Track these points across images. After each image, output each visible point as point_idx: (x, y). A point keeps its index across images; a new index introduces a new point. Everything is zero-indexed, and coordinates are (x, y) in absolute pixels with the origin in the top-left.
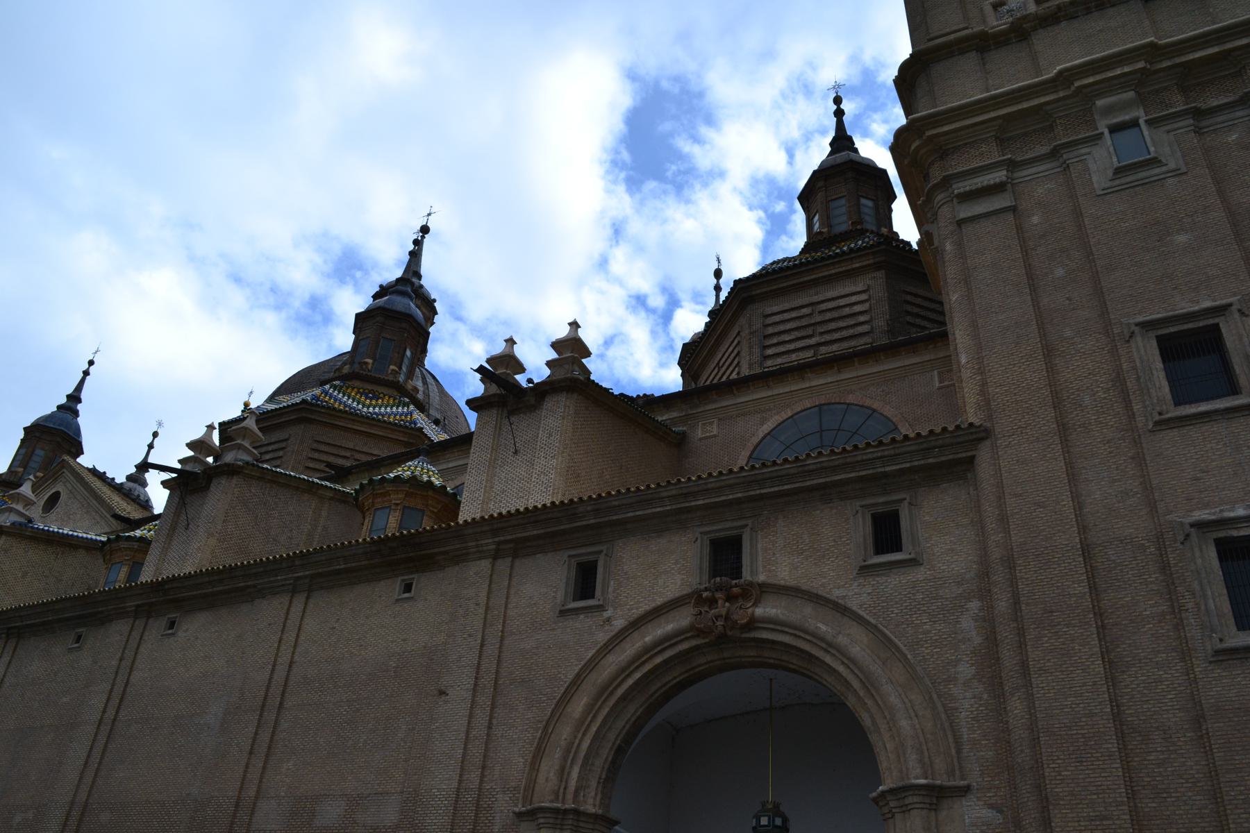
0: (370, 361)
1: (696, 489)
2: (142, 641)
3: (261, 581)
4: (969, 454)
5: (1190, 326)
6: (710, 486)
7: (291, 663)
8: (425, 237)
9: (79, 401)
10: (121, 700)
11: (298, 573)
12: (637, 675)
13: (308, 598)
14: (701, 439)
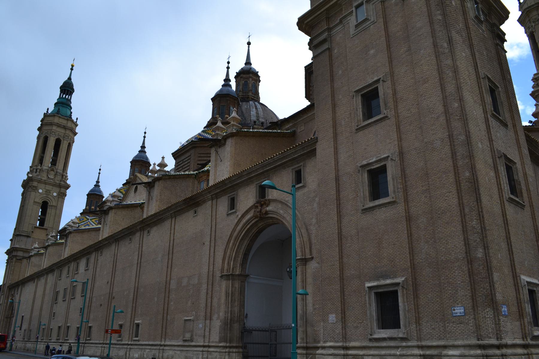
1: (250, 171)
4: (314, 147)
5: (370, 89)
6: (254, 169)
7: (174, 239)
9: (145, 147)
10: (141, 256)
12: (244, 232)
13: (175, 219)
14: (300, 132)
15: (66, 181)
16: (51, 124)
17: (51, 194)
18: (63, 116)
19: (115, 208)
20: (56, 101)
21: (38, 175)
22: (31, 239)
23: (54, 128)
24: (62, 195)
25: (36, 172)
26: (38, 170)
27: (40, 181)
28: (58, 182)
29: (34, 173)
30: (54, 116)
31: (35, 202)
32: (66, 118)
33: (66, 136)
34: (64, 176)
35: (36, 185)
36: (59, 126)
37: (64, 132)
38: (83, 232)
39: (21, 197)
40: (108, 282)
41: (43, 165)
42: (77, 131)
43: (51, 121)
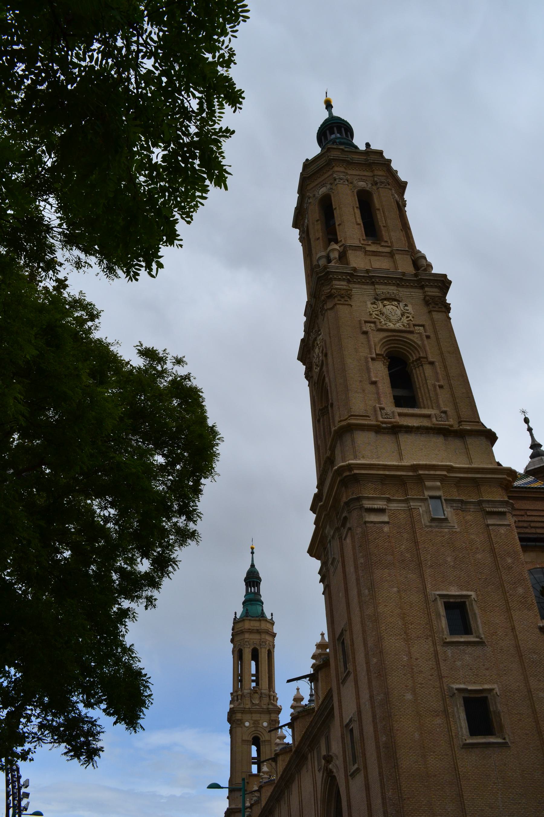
15: (275, 703)
16: (242, 632)
17: (260, 726)
18: (253, 617)
19: (281, 754)
21: (239, 704)
23: (247, 636)
25: (237, 700)
26: (239, 697)
28: (265, 707)
29: (236, 701)
30: (243, 620)
31: (243, 740)
32: (258, 619)
33: (263, 642)
35: (240, 718)
36: (251, 631)
42: (275, 631)
43: (241, 629)
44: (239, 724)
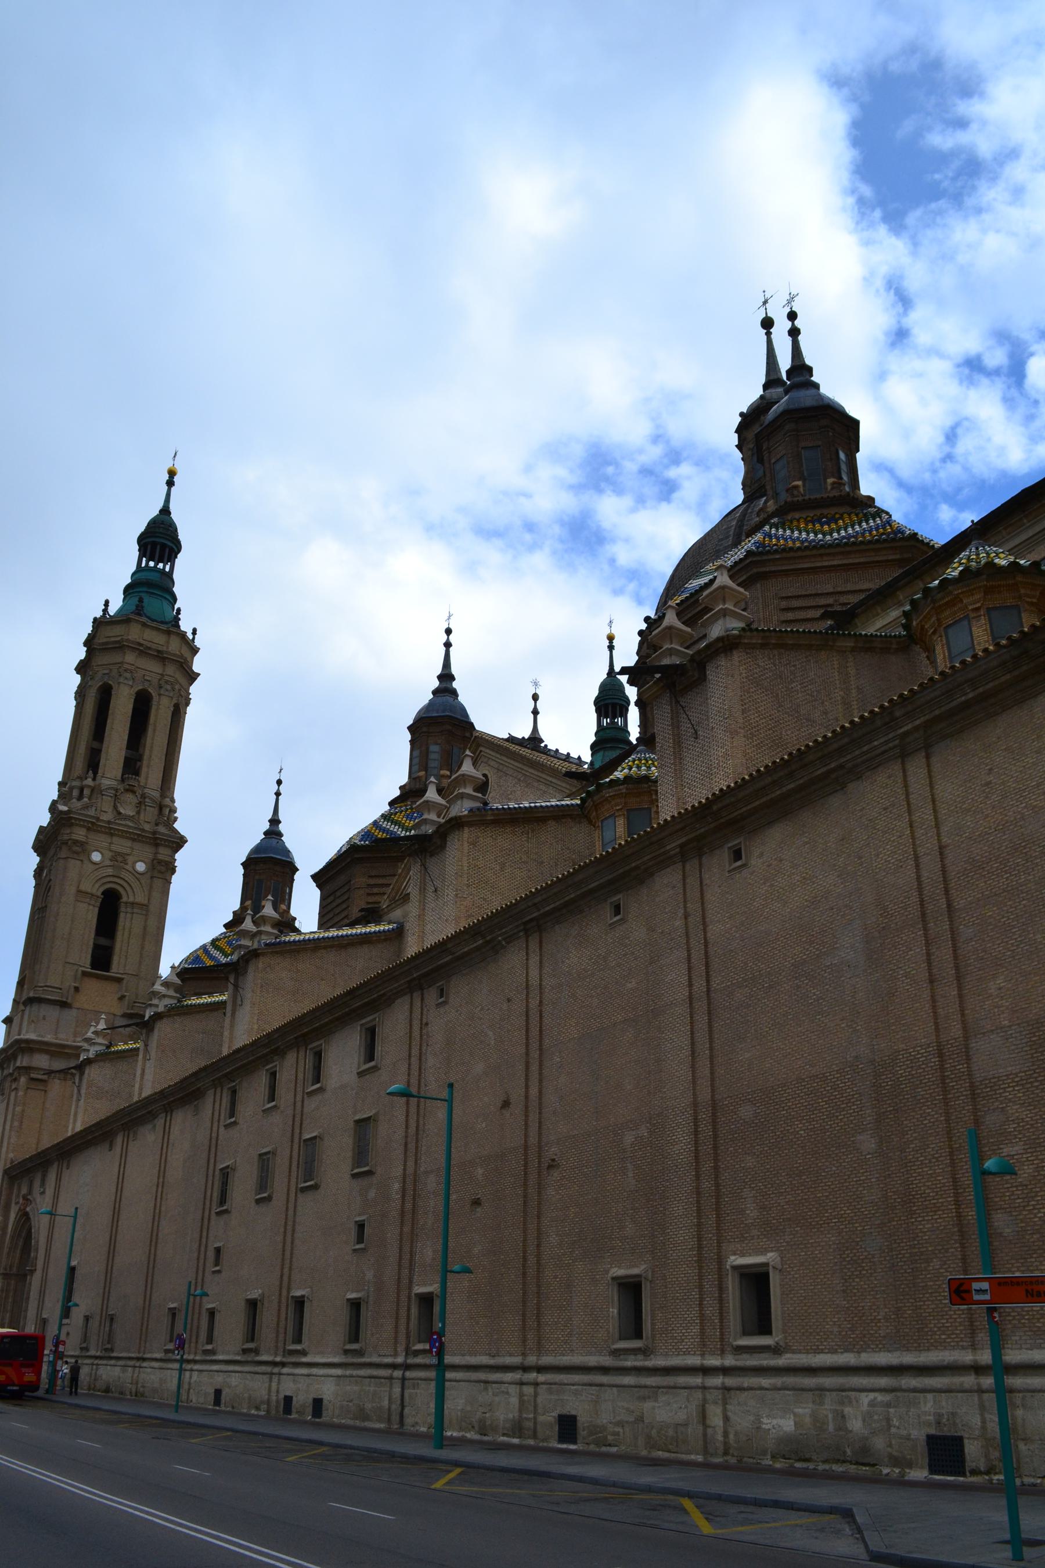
0: (800, 483)
2: (705, 887)
3: (849, 757)
8: (771, 333)
9: (452, 678)
10: (707, 965)
11: (901, 728)
16: (120, 647)
17: (127, 867)
18: (153, 620)
20: (129, 581)
21: (86, 807)
22: (74, 1012)
23: (130, 658)
24: (163, 869)
25: (80, 797)
26: (86, 792)
27: (93, 826)
28: (147, 827)
29: (74, 800)
31: (79, 891)
32: (163, 627)
33: (167, 682)
34: (166, 811)
35: (82, 839)
36: (142, 650)
37: (160, 672)
38: (298, 951)
39: (33, 883)
40: (506, 1104)
41: (100, 771)
42: (196, 668)
43: (118, 639)
44: (77, 853)
